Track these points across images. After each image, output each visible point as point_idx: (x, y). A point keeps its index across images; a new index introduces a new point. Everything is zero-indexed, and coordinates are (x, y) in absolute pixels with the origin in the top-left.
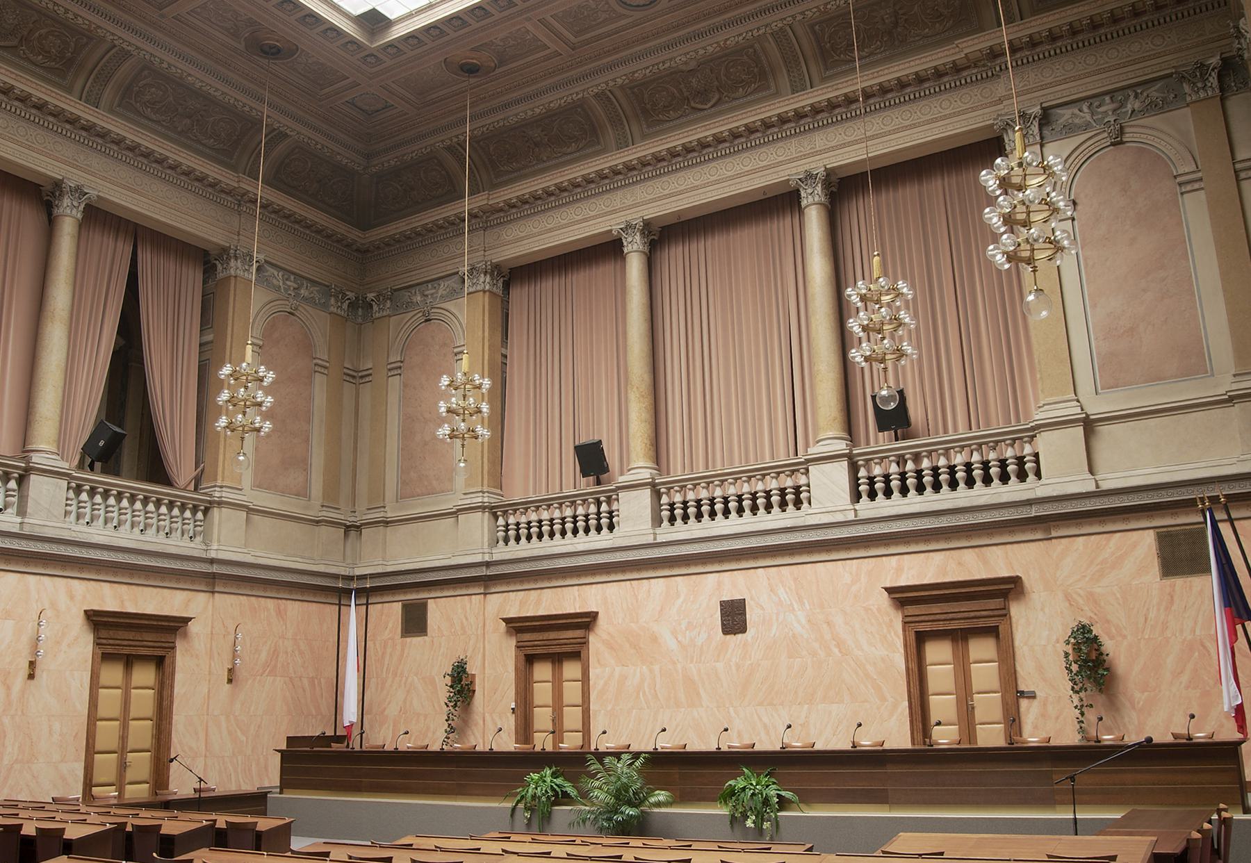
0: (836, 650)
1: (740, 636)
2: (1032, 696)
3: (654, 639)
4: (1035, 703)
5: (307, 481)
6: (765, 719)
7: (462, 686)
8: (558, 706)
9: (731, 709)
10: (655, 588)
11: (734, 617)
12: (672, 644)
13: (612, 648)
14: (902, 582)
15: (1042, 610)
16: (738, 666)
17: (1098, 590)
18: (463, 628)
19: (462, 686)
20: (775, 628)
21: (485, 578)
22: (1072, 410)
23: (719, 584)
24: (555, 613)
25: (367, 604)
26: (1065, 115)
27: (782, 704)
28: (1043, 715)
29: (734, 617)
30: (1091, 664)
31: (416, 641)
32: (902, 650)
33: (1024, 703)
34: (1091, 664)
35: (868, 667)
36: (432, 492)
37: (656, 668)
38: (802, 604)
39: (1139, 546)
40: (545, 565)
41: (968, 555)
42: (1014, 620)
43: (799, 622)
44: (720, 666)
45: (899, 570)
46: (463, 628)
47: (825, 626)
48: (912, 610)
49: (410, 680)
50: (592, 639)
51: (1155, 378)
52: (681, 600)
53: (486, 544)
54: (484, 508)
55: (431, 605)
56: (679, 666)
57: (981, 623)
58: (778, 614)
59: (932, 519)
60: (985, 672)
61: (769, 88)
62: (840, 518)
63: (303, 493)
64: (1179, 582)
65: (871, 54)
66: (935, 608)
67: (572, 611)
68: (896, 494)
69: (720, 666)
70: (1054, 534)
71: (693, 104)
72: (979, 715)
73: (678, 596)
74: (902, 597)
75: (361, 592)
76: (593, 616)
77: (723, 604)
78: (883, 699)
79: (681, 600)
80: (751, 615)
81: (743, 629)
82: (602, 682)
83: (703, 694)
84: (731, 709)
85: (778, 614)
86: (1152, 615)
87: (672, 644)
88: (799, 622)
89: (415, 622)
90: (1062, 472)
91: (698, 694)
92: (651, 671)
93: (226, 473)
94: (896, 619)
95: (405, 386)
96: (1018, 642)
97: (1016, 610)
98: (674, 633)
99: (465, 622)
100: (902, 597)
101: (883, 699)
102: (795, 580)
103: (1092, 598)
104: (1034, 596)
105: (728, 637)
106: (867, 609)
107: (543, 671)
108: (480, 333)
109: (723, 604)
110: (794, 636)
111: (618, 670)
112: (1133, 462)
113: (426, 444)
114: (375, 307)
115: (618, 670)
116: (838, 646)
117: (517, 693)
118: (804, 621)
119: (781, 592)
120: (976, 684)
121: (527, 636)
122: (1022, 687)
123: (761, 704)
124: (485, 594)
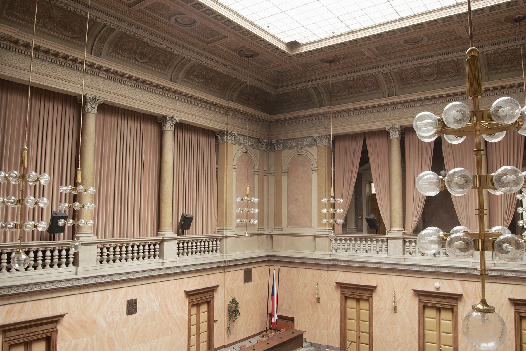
0: (167, 315)
1: (133, 315)
3: (94, 322)
10: (96, 297)
11: (132, 307)
12: (103, 323)
13: (71, 331)
23: (127, 292)
26: (239, 137)
29: (132, 307)
34: (233, 310)
38: (157, 298)
39: (240, 274)
40: (35, 289)
41: (206, 277)
43: (156, 306)
44: (124, 330)
45: (188, 283)
48: (191, 298)
50: (59, 327)
52: (109, 301)
56: (106, 333)
59: (202, 266)
60: (204, 316)
61: (165, 71)
62: (175, 265)
64: (246, 284)
65: (198, 82)
66: (198, 296)
69: (124, 330)
71: (136, 56)
73: (108, 300)
74: (189, 294)
77: (128, 301)
78: (180, 331)
79: (109, 301)
80: (139, 305)
83: (116, 344)
87: (103, 323)
88: (156, 306)
91: (114, 345)
94: (186, 301)
97: (215, 295)
100: (189, 294)
101: (180, 331)
109: (128, 301)
110: (154, 312)
111: (73, 341)
115: (73, 341)
116: (168, 314)
118: (158, 305)
119: (151, 294)
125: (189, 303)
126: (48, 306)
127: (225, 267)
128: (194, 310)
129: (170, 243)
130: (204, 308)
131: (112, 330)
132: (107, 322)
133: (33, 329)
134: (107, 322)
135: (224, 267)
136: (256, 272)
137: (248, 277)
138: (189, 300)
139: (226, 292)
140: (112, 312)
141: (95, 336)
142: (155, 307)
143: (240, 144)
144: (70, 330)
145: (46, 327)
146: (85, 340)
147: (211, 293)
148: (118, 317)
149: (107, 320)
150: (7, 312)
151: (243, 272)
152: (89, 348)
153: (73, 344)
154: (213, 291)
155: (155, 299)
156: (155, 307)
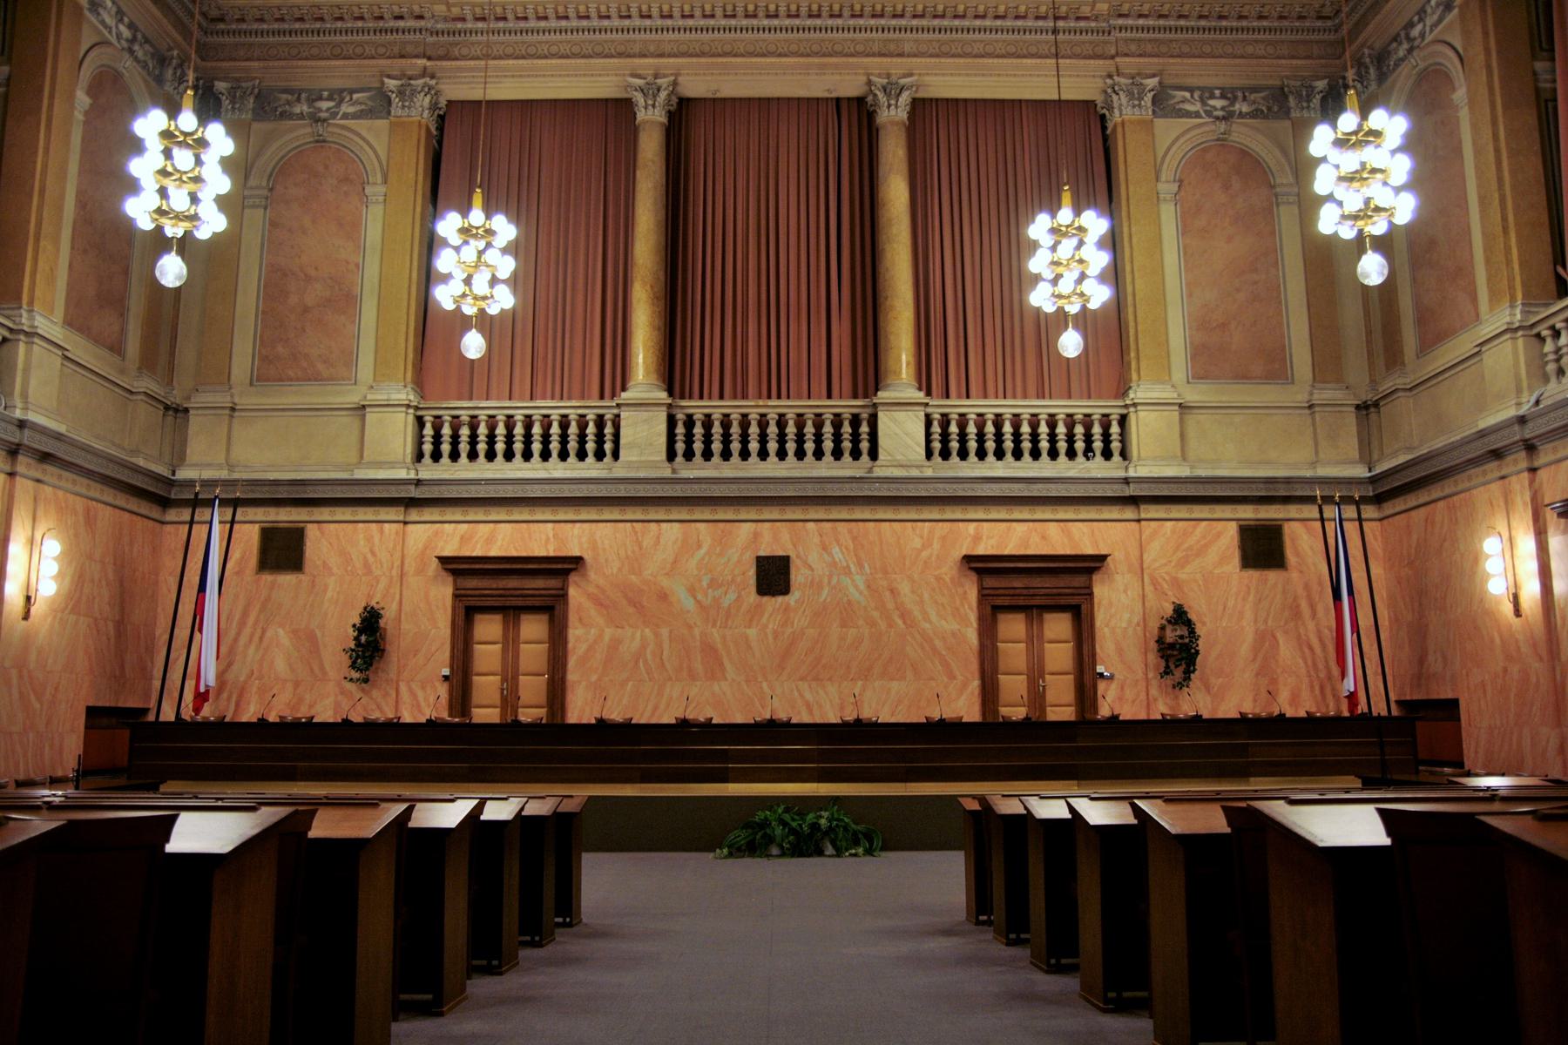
0: (900, 622)
1: (780, 599)
2: (1111, 678)
3: (663, 596)
4: (1114, 686)
5: (123, 331)
6: (808, 696)
7: (370, 642)
8: (510, 677)
9: (765, 685)
11: (773, 576)
12: (689, 603)
14: (981, 550)
15: (1125, 591)
16: (776, 635)
17: (1182, 576)
18: (366, 565)
19: (370, 642)
20: (825, 592)
21: (411, 500)
22: (1167, 394)
23: (756, 535)
24: (524, 554)
25: (191, 523)
27: (830, 679)
28: (1120, 699)
29: (773, 576)
30: (1178, 648)
31: (287, 579)
32: (975, 625)
33: (1101, 685)
35: (938, 643)
36: (317, 378)
37: (665, 632)
38: (860, 565)
42: (1096, 601)
43: (856, 587)
44: (752, 632)
45: (977, 539)
46: (366, 565)
47: (887, 593)
48: (990, 582)
49: (269, 634)
51: (1242, 376)
52: (703, 551)
53: (409, 459)
54: (408, 406)
55: (312, 532)
56: (697, 632)
57: (1062, 602)
58: (830, 577)
63: (117, 348)
67: (543, 553)
68: (1009, 457)
69: (752, 632)
70: (1143, 516)
72: (1051, 697)
73: (699, 547)
75: (224, 503)
76: (578, 560)
77: (760, 560)
79: (703, 551)
80: (798, 576)
81: (785, 590)
82: (583, 648)
84: (765, 685)
85: (830, 577)
86: (1231, 603)
88: (856, 587)
89: (283, 551)
90: (1153, 453)
91: (721, 664)
92: (657, 635)
93: (38, 293)
95: (274, 224)
96: (1098, 623)
97: (1100, 590)
98: (692, 591)
99: (371, 559)
101: (952, 677)
102: (854, 539)
103: (1176, 583)
104: (1118, 578)
105: (765, 599)
106: (938, 579)
107: (488, 628)
108: (412, 175)
109: (760, 560)
110: (849, 602)
112: (1227, 454)
113: (306, 310)
114: (226, 103)
115: (609, 633)
116: (902, 616)
117: (452, 657)
118: (862, 586)
119: (836, 550)
120: (1050, 665)
121: (473, 583)
122: (1100, 669)
123: (802, 679)
124: (406, 523)
125: (983, 596)
126: (548, 539)
127: (1134, 499)
128: (1013, 626)
129: (901, 415)
130: (1058, 626)
131: (714, 625)
132: (698, 602)
133: (513, 583)
134: (698, 602)
135: (1134, 501)
136: (1303, 539)
137: (1262, 548)
138: (981, 589)
139: (1149, 588)
140: (712, 580)
141: (665, 632)
142: (852, 590)
143: (1197, 115)
144: (599, 603)
145: (539, 583)
146: (638, 634)
147: (1078, 581)
148: (731, 597)
149: (699, 597)
150: (462, 538)
151: (1232, 530)
152: (649, 657)
153: (607, 638)
154: (1091, 571)
155: (853, 569)
156: (852, 590)
